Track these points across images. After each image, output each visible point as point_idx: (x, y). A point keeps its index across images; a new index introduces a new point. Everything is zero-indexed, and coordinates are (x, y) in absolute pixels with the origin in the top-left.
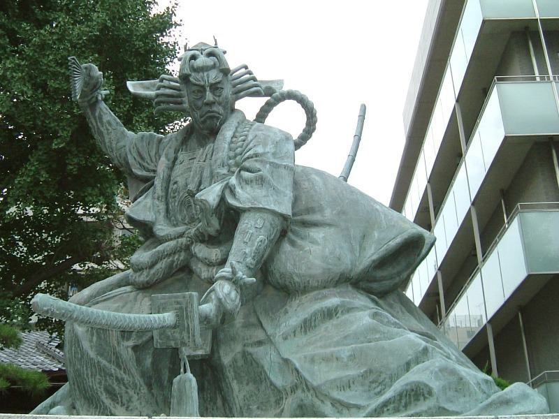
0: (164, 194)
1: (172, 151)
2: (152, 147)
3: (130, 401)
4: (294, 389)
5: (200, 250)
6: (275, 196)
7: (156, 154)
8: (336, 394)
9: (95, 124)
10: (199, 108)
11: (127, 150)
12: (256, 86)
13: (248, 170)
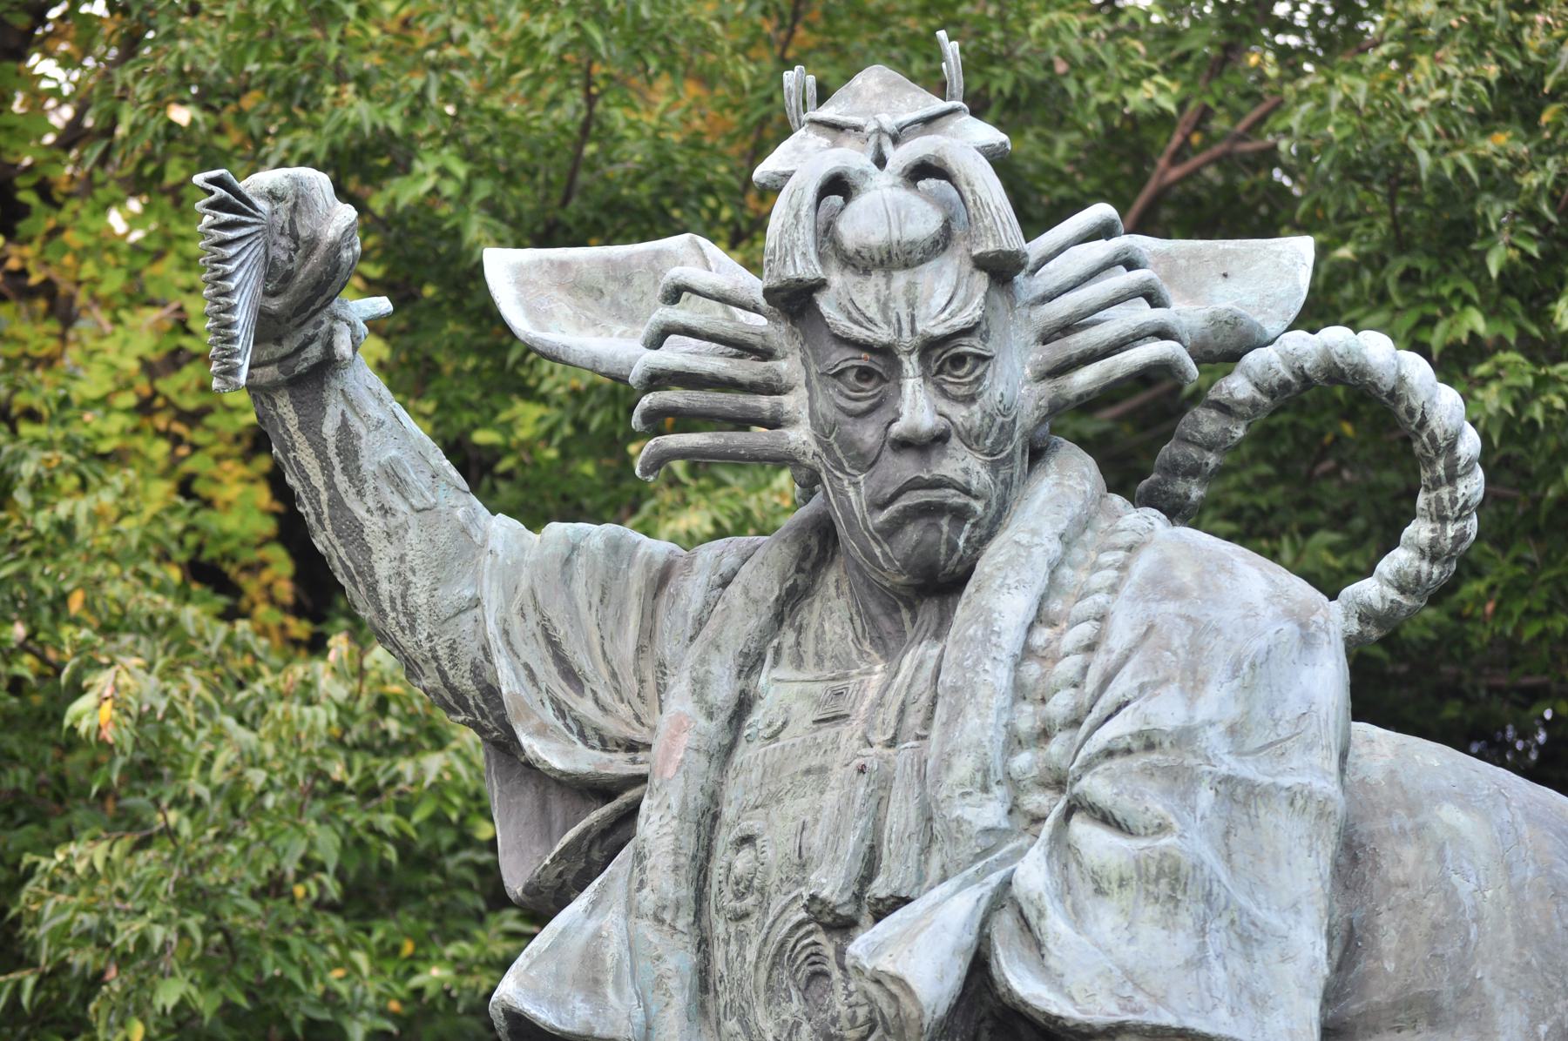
0: (687, 892)
2: (620, 620)
6: (1236, 963)
7: (640, 649)
9: (318, 480)
10: (866, 462)
11: (492, 629)
12: (1163, 333)
13: (1106, 819)
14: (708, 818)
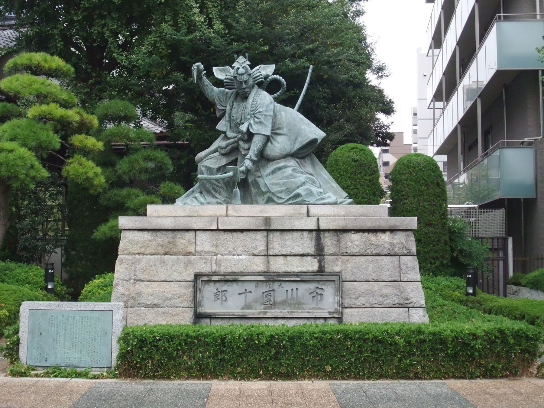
1: (231, 103)
3: (220, 192)
4: (267, 192)
5: (241, 143)
8: (279, 195)
12: (262, 78)
13: (257, 118)
14: (230, 114)
